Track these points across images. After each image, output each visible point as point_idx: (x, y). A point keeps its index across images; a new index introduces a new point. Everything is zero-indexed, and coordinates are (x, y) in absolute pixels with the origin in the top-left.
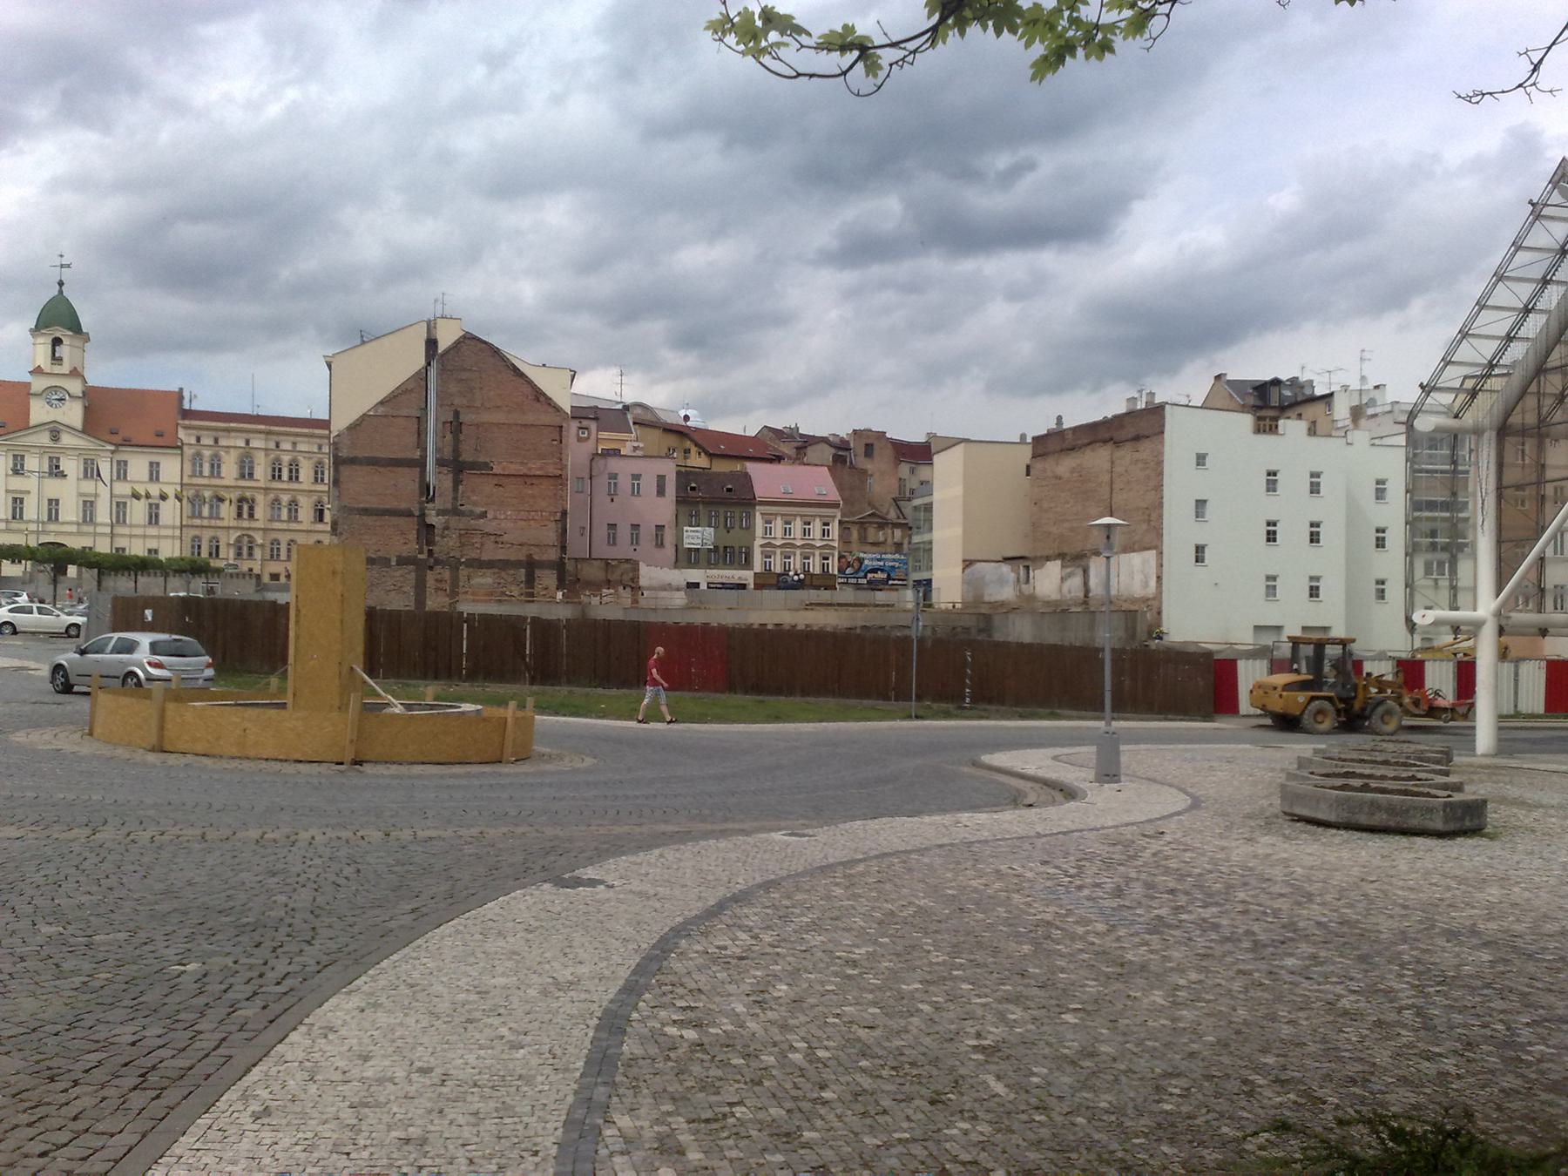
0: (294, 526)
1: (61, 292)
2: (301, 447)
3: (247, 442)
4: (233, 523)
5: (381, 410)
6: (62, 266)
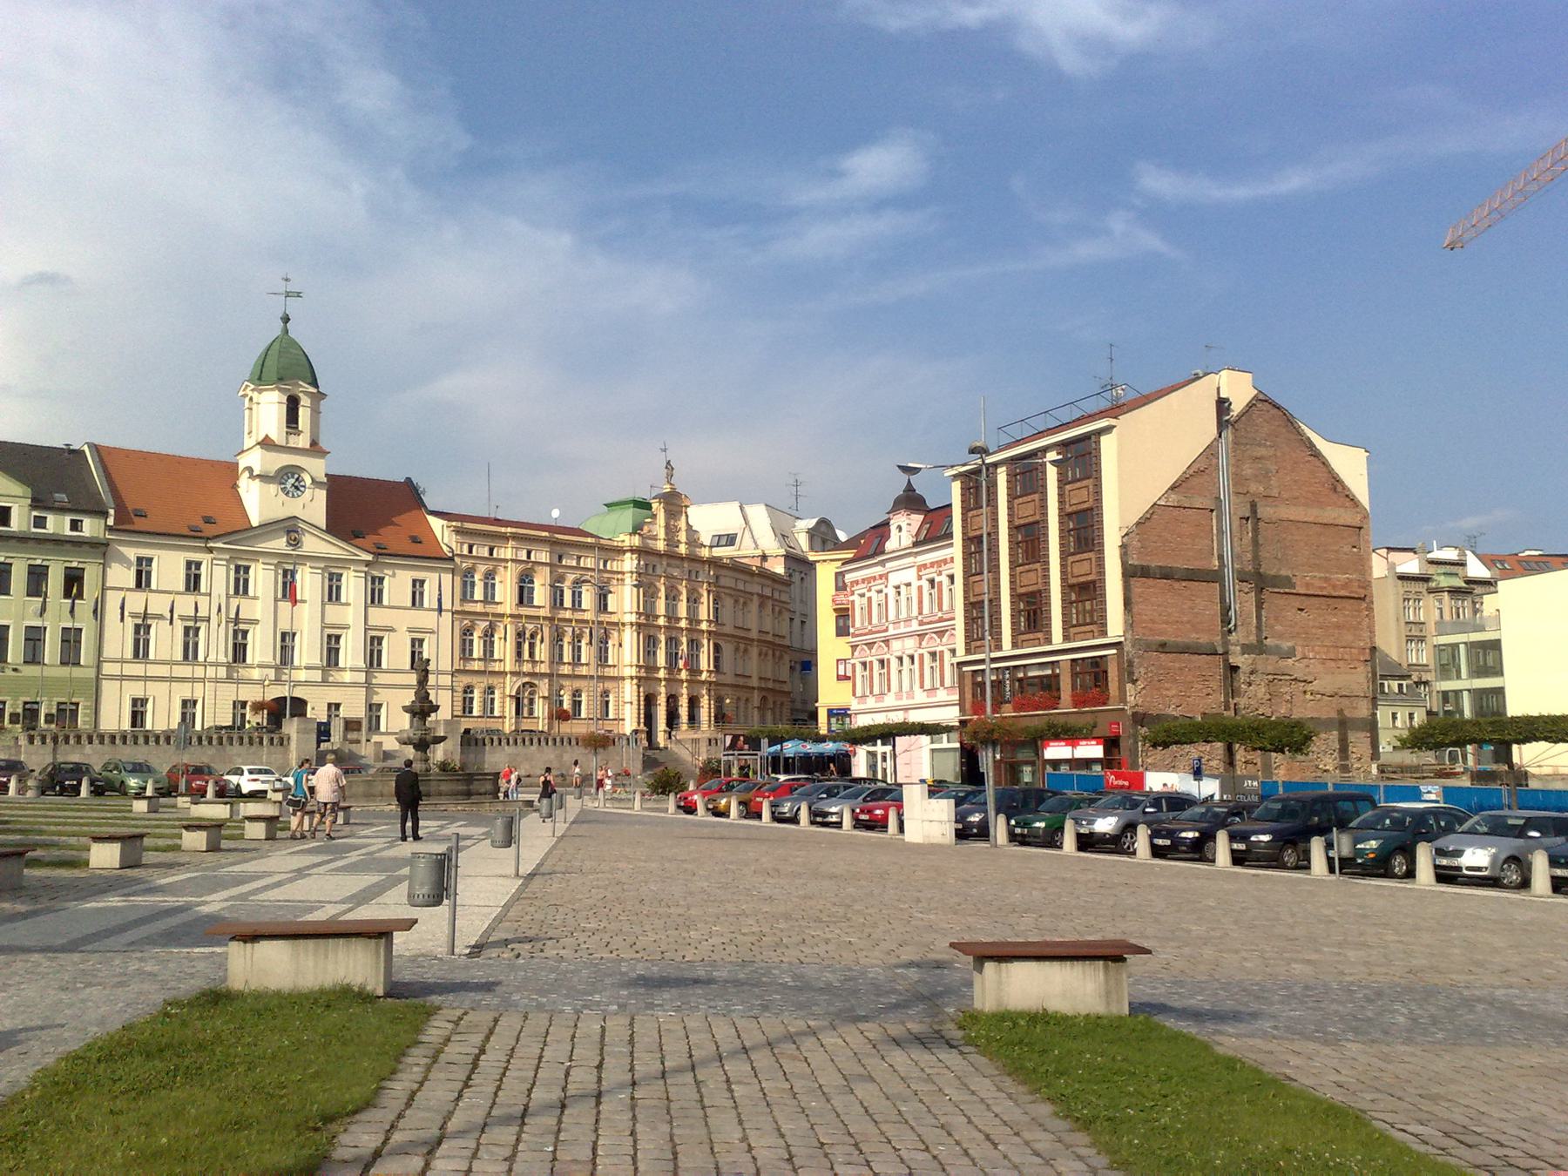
1: (286, 331)
5: (1174, 499)
6: (288, 295)
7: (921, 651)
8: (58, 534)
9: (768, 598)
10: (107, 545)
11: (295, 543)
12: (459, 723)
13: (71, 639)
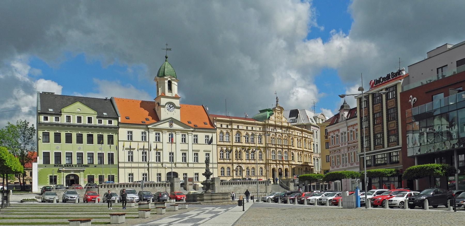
0: (253, 162)
2: (254, 129)
4: (235, 161)
9: (307, 138)
10: (119, 128)
12: (219, 178)
13: (111, 156)
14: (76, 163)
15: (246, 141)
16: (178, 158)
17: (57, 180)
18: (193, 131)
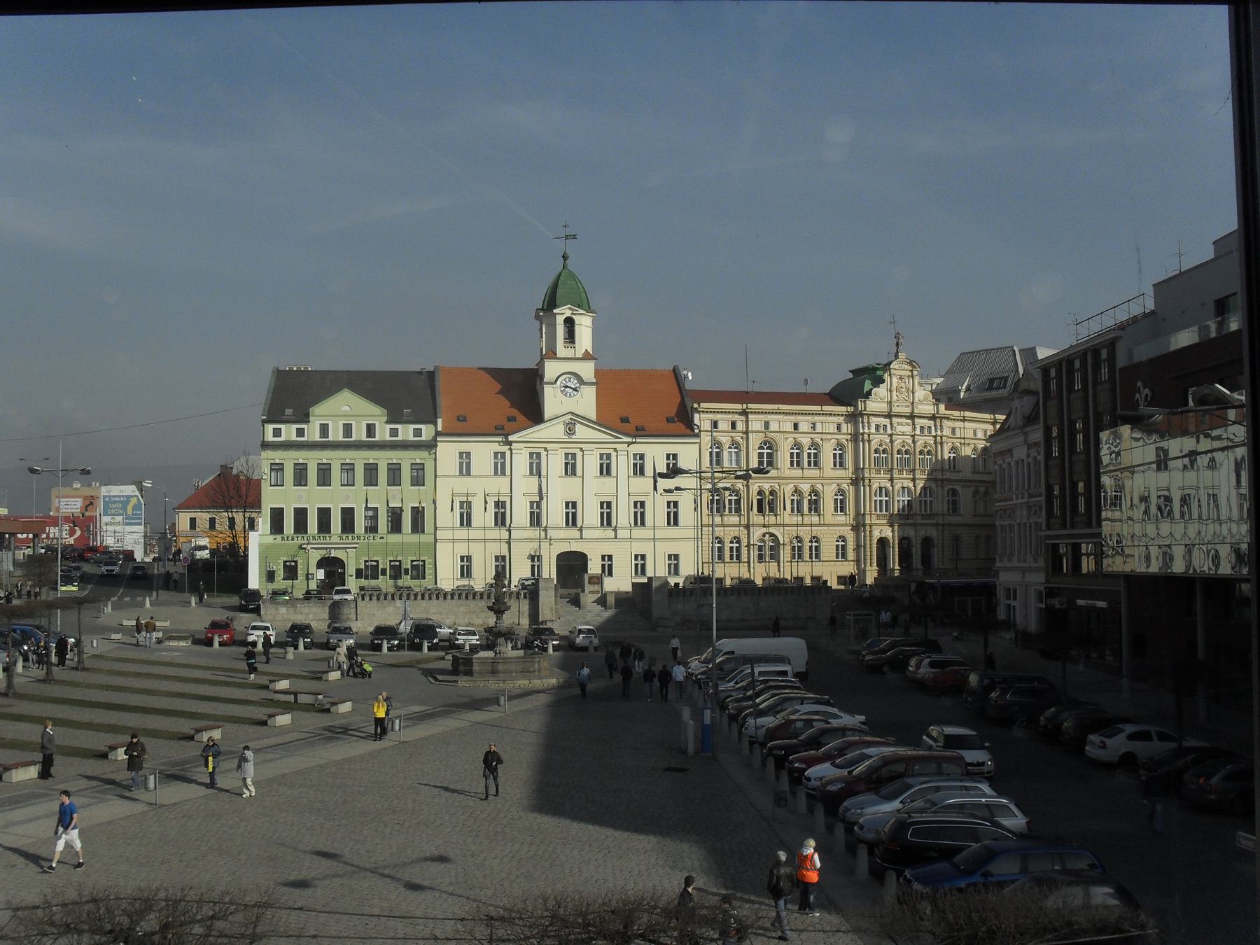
3: (767, 425)
6: (567, 238)
7: (1031, 521)
8: (406, 440)
11: (570, 430)
14: (338, 531)
15: (792, 463)
16: (590, 514)
17: (299, 569)
18: (629, 444)
